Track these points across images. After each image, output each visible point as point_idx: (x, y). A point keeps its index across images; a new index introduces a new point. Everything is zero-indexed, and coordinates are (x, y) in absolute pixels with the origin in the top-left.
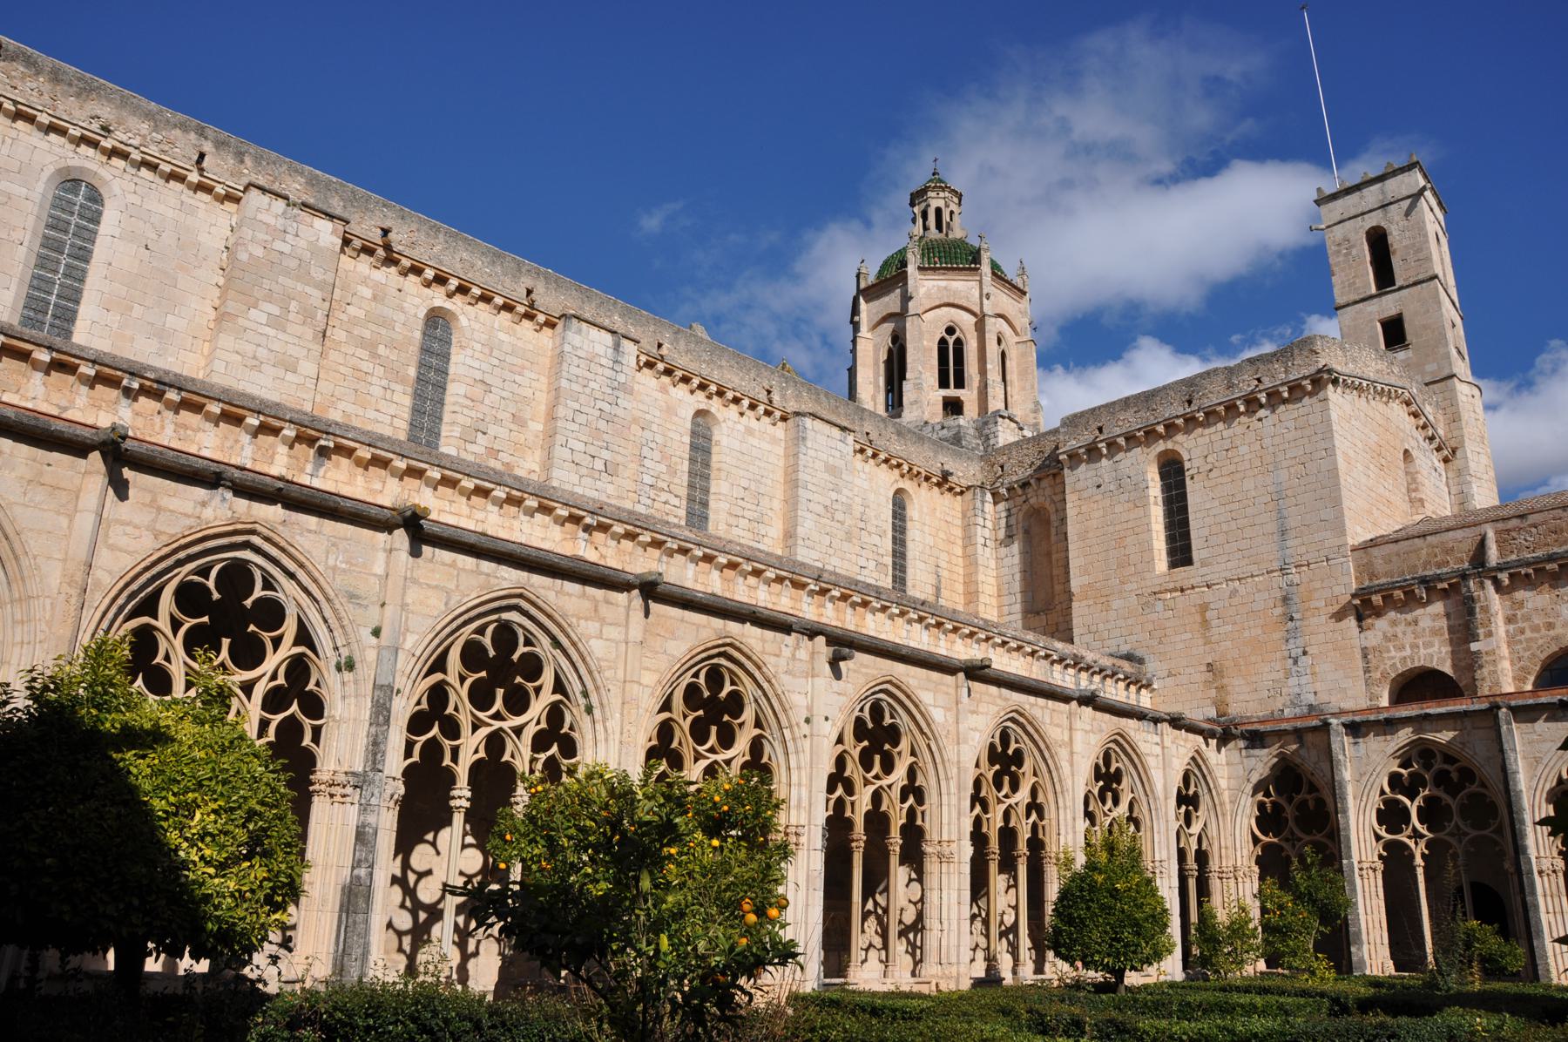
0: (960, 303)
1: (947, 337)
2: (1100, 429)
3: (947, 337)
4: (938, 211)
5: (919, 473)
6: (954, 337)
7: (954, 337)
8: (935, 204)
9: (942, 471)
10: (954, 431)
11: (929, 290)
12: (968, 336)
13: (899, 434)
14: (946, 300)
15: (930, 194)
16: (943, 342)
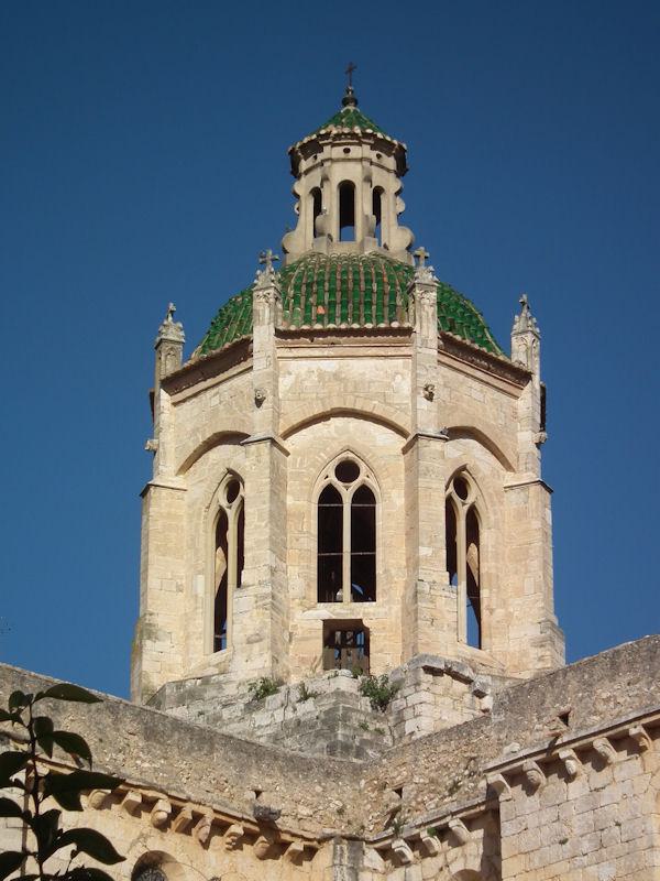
0: (368, 409)
1: (339, 485)
2: (565, 718)
3: (339, 485)
4: (347, 190)
5: (197, 817)
6: (355, 485)
7: (355, 485)
8: (339, 173)
9: (256, 809)
10: (327, 704)
11: (299, 382)
12: (386, 482)
13: (150, 734)
14: (337, 404)
15: (328, 152)
16: (329, 496)
